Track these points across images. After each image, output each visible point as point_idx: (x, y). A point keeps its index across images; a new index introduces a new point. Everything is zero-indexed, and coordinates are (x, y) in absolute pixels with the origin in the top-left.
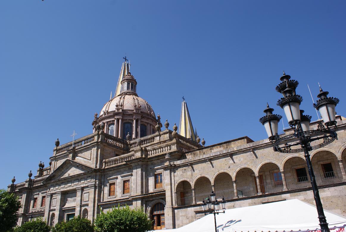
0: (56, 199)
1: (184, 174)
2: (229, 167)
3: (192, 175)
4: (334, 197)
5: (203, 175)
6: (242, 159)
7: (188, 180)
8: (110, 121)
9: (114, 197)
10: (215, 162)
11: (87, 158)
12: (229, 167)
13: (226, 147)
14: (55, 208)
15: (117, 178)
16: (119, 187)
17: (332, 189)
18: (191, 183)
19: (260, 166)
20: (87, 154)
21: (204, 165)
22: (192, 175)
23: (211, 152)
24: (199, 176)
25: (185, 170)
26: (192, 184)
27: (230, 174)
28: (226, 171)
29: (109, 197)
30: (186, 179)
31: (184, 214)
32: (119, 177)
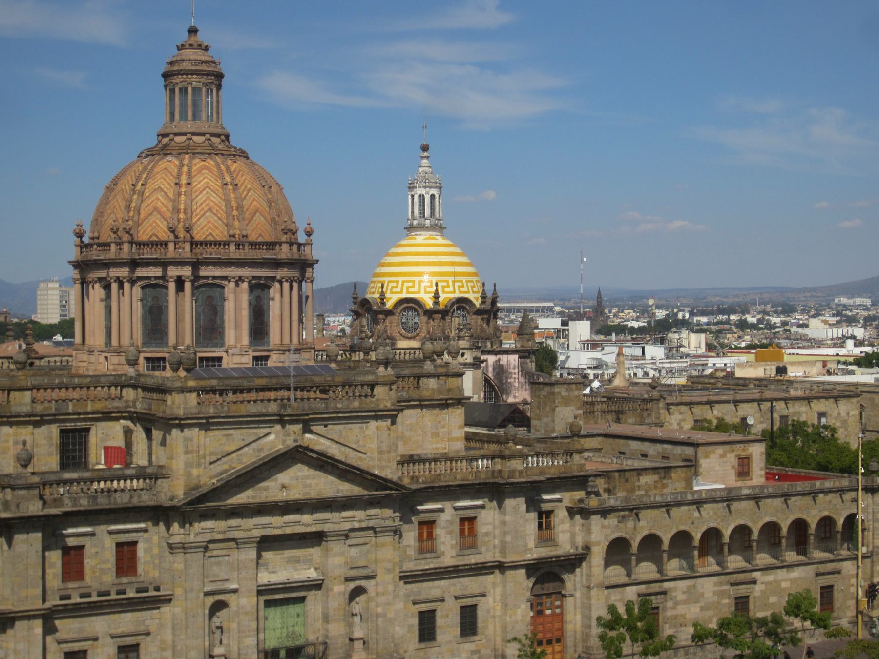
0: (226, 558)
1: (621, 525)
2: (693, 523)
3: (635, 528)
4: (801, 578)
5: (653, 531)
6: (711, 513)
7: (628, 537)
8: (259, 278)
9: (433, 555)
10: (675, 511)
11: (354, 446)
12: (693, 523)
13: (662, 475)
14: (234, 586)
15: (441, 510)
16: (450, 533)
17: (801, 568)
18: (632, 542)
19: (732, 527)
20: (352, 432)
21: (655, 512)
22: (635, 528)
23: (639, 480)
24: (645, 532)
25: (624, 517)
26: (635, 545)
27: (693, 534)
28: (687, 528)
29: (420, 556)
30: (624, 535)
31: (618, 598)
32: (448, 505)
